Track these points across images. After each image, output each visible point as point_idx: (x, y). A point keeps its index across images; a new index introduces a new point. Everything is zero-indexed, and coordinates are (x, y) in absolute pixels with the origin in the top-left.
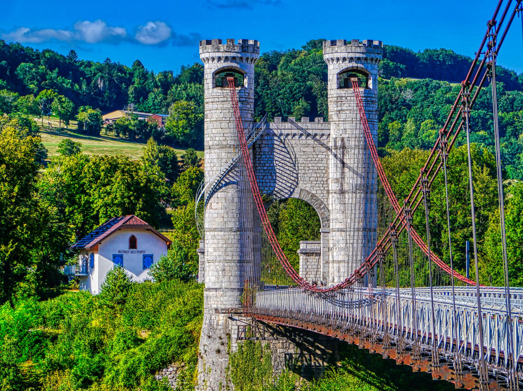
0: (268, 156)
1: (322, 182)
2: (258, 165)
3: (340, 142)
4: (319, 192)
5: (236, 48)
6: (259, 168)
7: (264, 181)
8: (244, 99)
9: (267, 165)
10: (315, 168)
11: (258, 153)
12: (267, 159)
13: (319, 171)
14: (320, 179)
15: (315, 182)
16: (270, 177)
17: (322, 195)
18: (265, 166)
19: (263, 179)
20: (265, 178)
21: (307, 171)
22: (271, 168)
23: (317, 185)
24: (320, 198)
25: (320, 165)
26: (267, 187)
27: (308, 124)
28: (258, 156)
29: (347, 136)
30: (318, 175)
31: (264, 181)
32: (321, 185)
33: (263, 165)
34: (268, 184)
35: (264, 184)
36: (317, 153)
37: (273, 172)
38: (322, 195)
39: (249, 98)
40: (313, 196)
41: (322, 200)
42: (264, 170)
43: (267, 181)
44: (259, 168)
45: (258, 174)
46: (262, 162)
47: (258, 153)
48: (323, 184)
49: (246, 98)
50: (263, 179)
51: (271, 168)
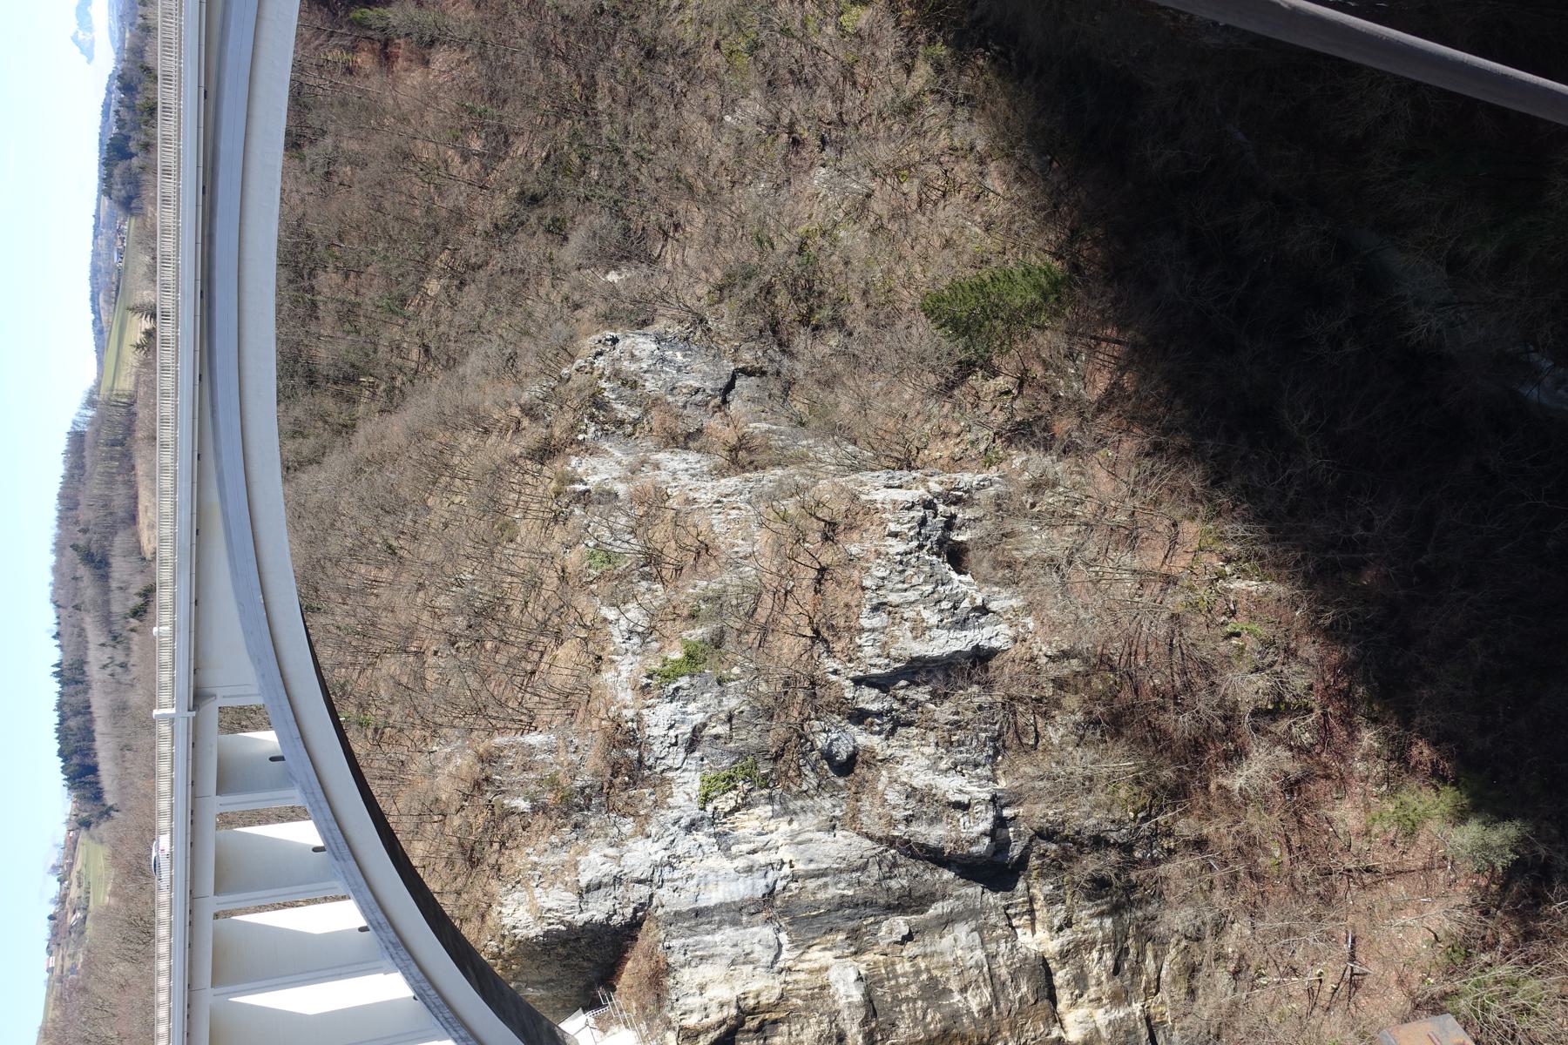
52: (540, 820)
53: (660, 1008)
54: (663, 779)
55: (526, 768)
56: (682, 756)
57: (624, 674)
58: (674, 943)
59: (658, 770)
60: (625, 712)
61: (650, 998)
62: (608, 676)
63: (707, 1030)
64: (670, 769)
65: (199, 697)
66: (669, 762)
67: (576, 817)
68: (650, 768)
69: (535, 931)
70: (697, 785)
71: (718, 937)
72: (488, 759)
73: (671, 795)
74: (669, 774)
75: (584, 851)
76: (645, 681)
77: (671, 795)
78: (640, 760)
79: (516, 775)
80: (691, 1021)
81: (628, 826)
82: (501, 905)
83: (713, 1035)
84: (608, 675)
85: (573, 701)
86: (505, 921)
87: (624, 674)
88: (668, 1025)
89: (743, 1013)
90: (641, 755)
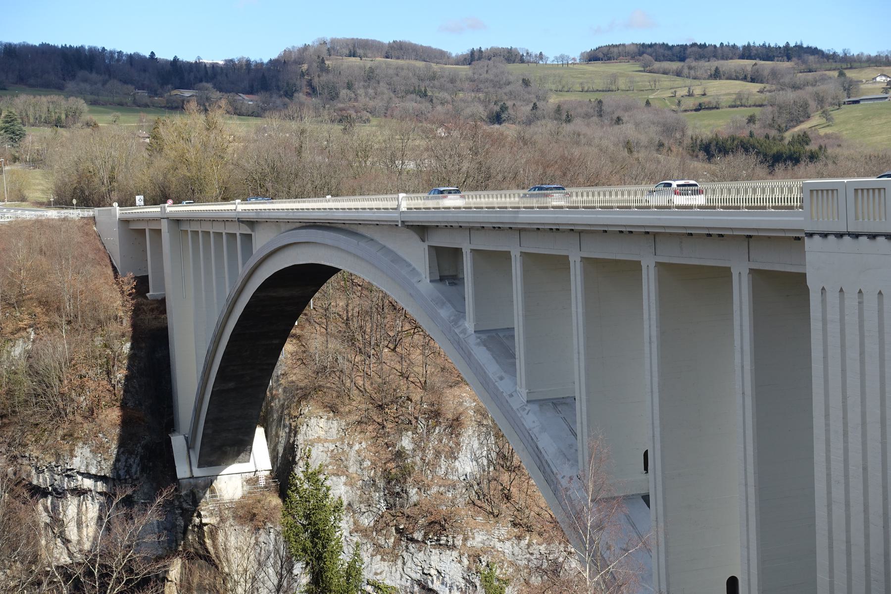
52: (386, 455)
53: (234, 518)
54: (397, 556)
55: (437, 454)
56: (414, 576)
57: (499, 545)
58: (272, 536)
59: (404, 554)
60: (460, 537)
61: (241, 512)
62: (504, 530)
63: (215, 546)
64: (404, 563)
65: (252, 223)
66: (409, 564)
67: (381, 484)
68: (407, 547)
69: (300, 438)
70: (388, 582)
71: (271, 571)
72: (455, 425)
73: (383, 559)
74: (399, 562)
75: (350, 484)
76: (484, 559)
77: (383, 559)
78: (412, 540)
79: (433, 443)
80: (221, 538)
81: (367, 521)
82: (328, 419)
83: (211, 549)
84: (503, 531)
85: (489, 498)
86: (313, 421)
87: (499, 545)
88: (222, 520)
89: (226, 577)
90: (417, 541)
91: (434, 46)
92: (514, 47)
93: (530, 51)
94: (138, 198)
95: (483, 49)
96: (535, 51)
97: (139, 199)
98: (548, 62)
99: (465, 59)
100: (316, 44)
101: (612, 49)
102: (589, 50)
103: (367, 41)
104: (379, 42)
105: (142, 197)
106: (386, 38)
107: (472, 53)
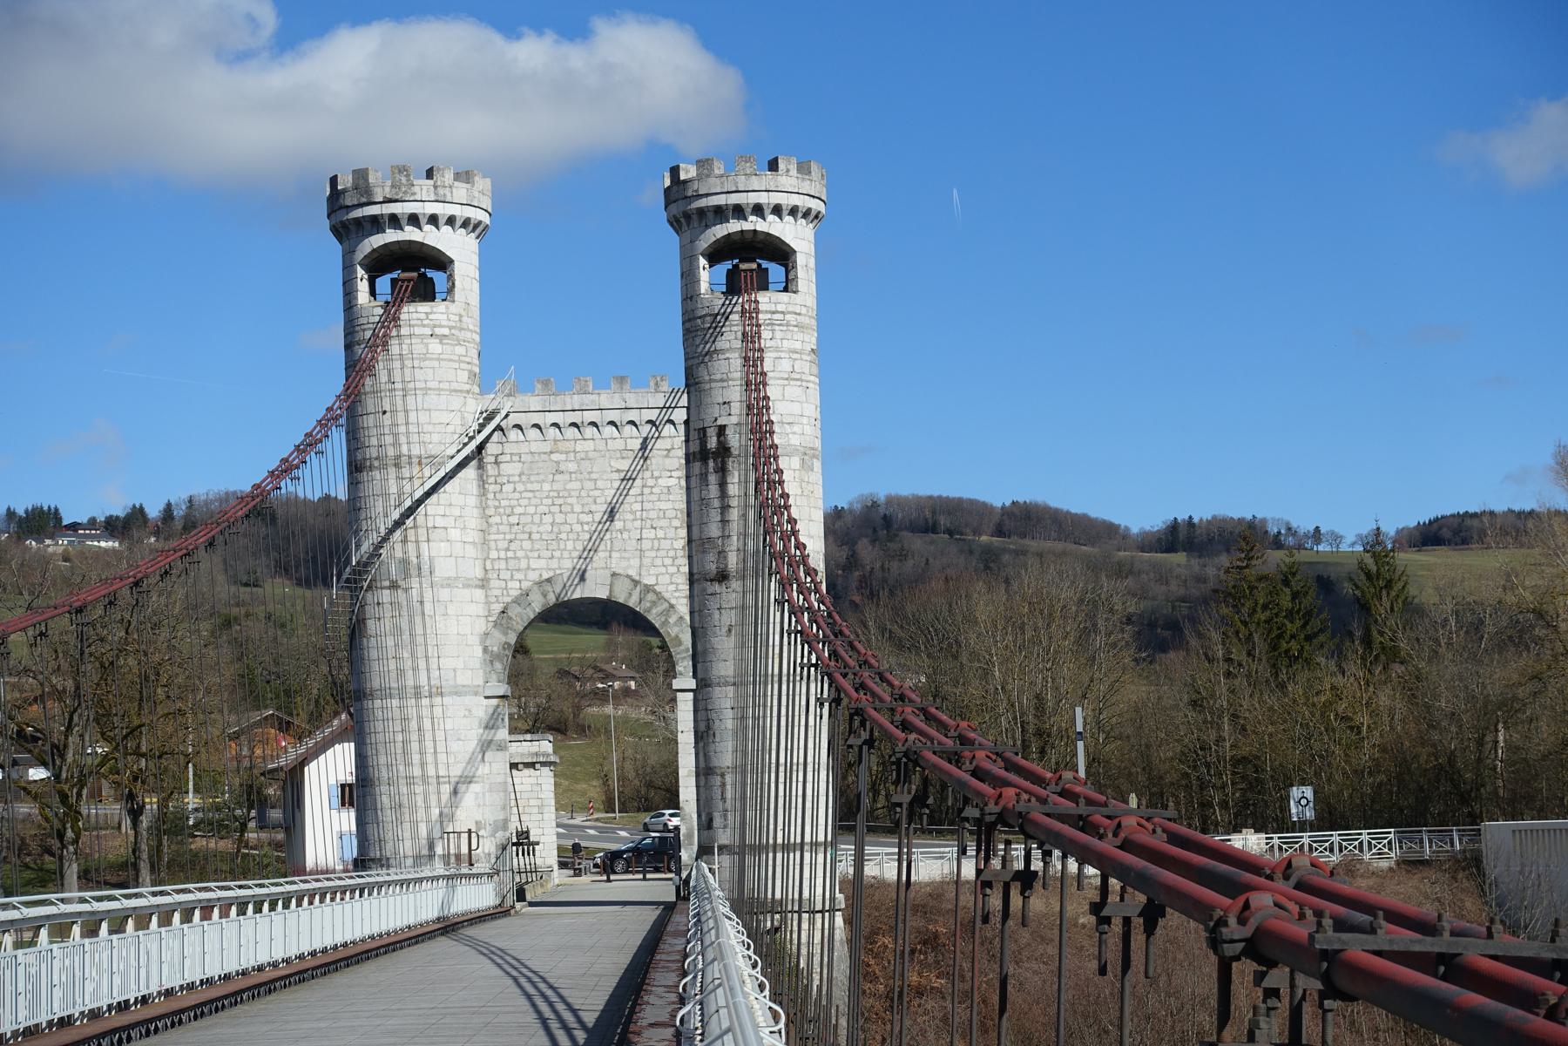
0: (520, 487)
1: (672, 553)
2: (491, 511)
3: (715, 439)
4: (667, 579)
5: (416, 189)
6: (497, 519)
7: (510, 554)
8: (446, 331)
9: (518, 510)
10: (653, 514)
11: (492, 480)
12: (517, 495)
13: (663, 523)
14: (666, 544)
15: (653, 554)
16: (527, 545)
17: (672, 588)
18: (513, 514)
19: (507, 549)
20: (513, 546)
21: (629, 525)
22: (529, 519)
23: (658, 562)
24: (667, 595)
25: (663, 506)
26: (518, 570)
27: (627, 396)
28: (491, 488)
29: (734, 420)
30: (660, 534)
31: (510, 554)
32: (668, 561)
33: (508, 511)
34: (524, 564)
35: (512, 563)
36: (656, 474)
37: (535, 529)
38: (672, 588)
39: (461, 329)
40: (648, 589)
41: (673, 601)
42: (511, 525)
43: (519, 554)
44: (497, 519)
45: (493, 537)
46: (503, 503)
47: (492, 480)
48: (674, 559)
49: (451, 328)
50: (507, 549)
51: (529, 519)
91: (1093, 514)
92: (1259, 516)
93: (1294, 525)
94: (1295, 792)
95: (1196, 520)
96: (1305, 525)
97: (1301, 801)
98: (1344, 548)
99: (1159, 540)
100: (857, 507)
101: (1468, 522)
102: (1413, 524)
103: (960, 500)
104: (984, 504)
105: (1308, 792)
106: (998, 495)
107: (1174, 527)
